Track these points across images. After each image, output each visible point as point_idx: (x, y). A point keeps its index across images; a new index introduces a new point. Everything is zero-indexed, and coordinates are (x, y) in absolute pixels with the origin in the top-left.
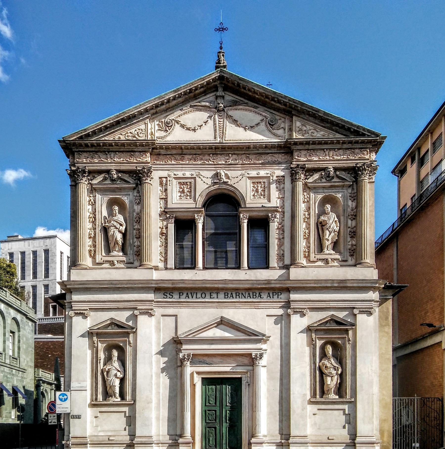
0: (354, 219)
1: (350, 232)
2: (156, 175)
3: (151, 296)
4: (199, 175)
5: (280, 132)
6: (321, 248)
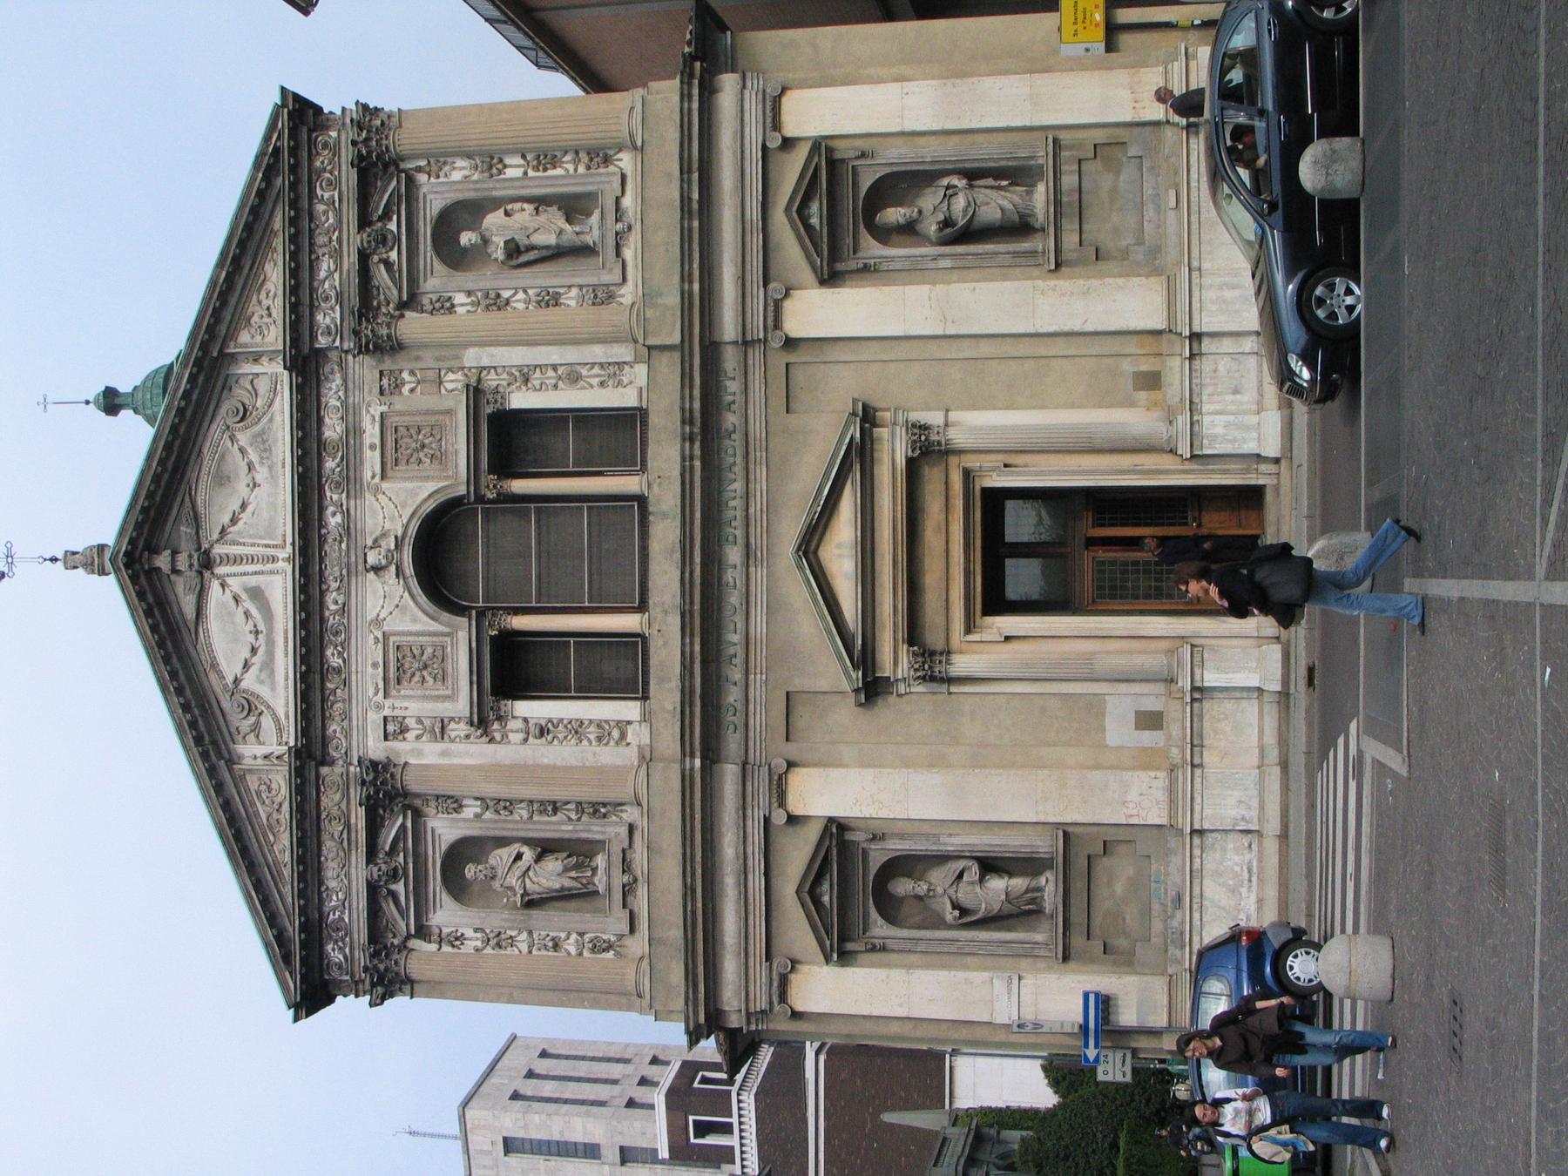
0: (501, 161)
1: (536, 169)
2: (376, 748)
3: (729, 774)
4: (377, 622)
5: (263, 386)
6: (583, 251)
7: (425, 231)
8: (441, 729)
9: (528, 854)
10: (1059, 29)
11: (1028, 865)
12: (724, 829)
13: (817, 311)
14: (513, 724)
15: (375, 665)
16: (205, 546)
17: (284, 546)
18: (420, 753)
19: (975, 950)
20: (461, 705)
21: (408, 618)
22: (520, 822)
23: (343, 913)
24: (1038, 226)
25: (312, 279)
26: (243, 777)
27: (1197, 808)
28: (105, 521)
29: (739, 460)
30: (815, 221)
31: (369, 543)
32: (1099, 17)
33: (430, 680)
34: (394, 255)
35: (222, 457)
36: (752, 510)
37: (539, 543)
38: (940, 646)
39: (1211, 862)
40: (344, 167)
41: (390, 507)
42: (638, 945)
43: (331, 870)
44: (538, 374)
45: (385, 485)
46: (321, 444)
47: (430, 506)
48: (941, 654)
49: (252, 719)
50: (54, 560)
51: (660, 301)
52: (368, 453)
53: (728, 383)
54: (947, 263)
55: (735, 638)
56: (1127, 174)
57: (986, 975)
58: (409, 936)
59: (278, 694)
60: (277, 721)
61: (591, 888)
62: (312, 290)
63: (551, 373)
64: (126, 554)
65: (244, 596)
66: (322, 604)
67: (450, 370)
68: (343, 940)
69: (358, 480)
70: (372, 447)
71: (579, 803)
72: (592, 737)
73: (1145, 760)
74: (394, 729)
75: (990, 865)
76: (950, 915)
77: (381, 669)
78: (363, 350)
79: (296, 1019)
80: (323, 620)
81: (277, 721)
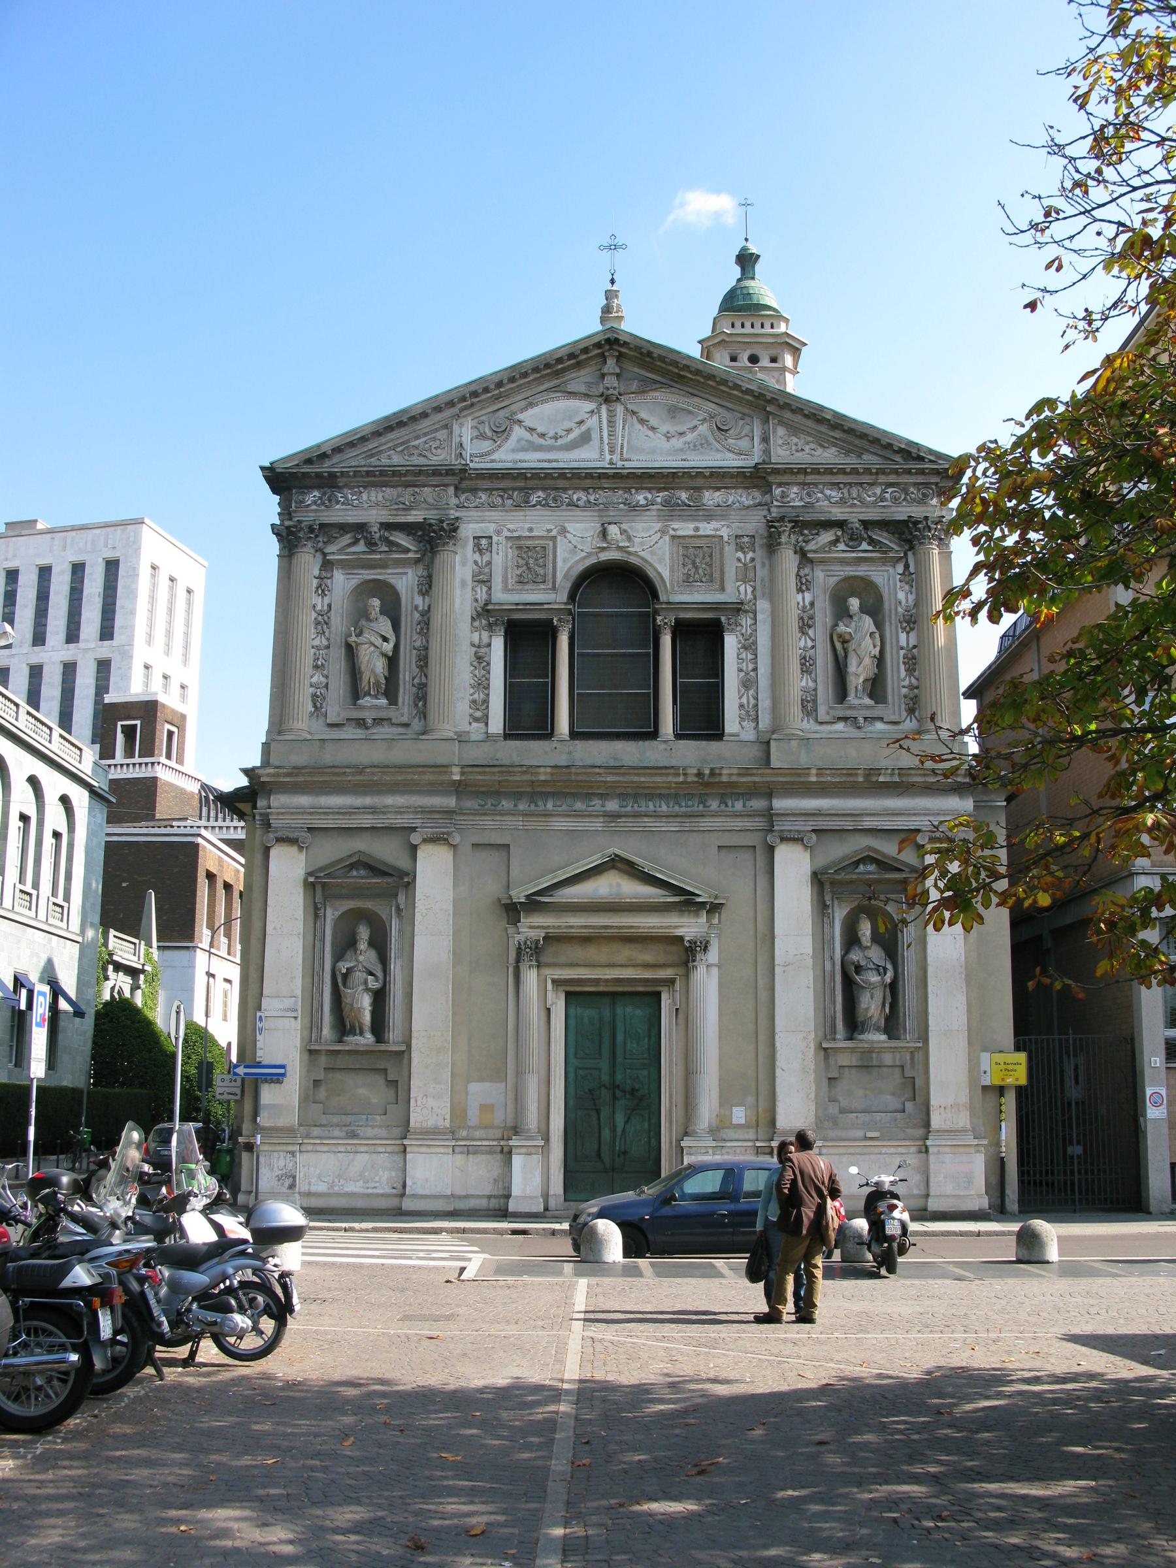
0: (912, 629)
2: (468, 530)
3: (451, 802)
4: (564, 531)
5: (744, 444)
6: (841, 692)
7: (861, 571)
8: (483, 579)
9: (388, 647)
10: (1001, 1052)
11: (379, 1026)
12: (406, 797)
13: (793, 869)
14: (485, 634)
15: (531, 530)
16: (622, 398)
17: (621, 460)
18: (464, 563)
19: (316, 984)
20: (500, 596)
21: (567, 555)
22: (410, 639)
23: (343, 504)
24: (856, 1035)
25: (824, 484)
26: (446, 427)
27: (423, 1149)
28: (640, 324)
29: (684, 809)
30: (861, 868)
31: (624, 526)
32: (1010, 1081)
33: (518, 572)
34: (841, 546)
35: (690, 412)
36: (646, 819)
37: (624, 655)
38: (543, 959)
39: (382, 1159)
40: (908, 509)
41: (650, 542)
42: (318, 729)
43: (376, 495)
44: (750, 656)
45: (667, 538)
46: (698, 489)
47: (651, 574)
48: (537, 961)
49: (489, 434)
50: (613, 282)
51: (803, 752)
52: (692, 526)
53: (741, 802)
54: (828, 967)
55: (550, 806)
56: (892, 1102)
57: (299, 993)
58: (325, 555)
59: (507, 455)
60: (489, 453)
61: (361, 694)
62: (815, 484)
63: (751, 667)
64: (617, 340)
65: (584, 428)
66: (576, 489)
67: (754, 589)
68: (323, 504)
69: (671, 518)
70: (697, 529)
71: (425, 685)
72: (476, 696)
73: (458, 1112)
74: (482, 544)
75: (380, 998)
76: (343, 967)
77: (528, 534)
78: (770, 524)
79: (262, 468)
80: (565, 490)
81: (489, 453)
